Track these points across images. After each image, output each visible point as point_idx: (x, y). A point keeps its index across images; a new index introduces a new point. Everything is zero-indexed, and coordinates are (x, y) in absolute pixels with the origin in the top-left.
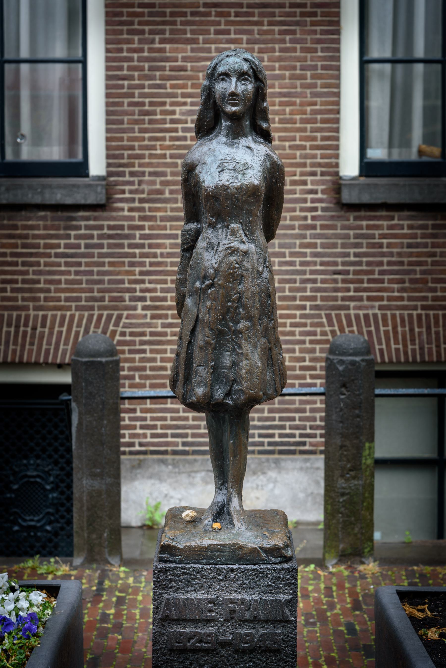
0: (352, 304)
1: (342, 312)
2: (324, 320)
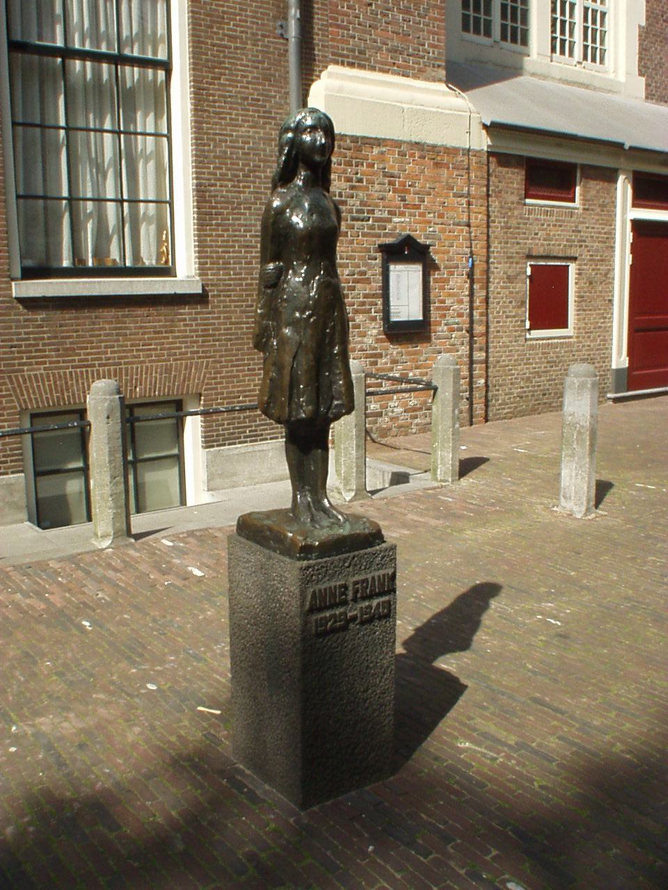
0: (25, 368)
1: (19, 374)
2: (7, 380)
